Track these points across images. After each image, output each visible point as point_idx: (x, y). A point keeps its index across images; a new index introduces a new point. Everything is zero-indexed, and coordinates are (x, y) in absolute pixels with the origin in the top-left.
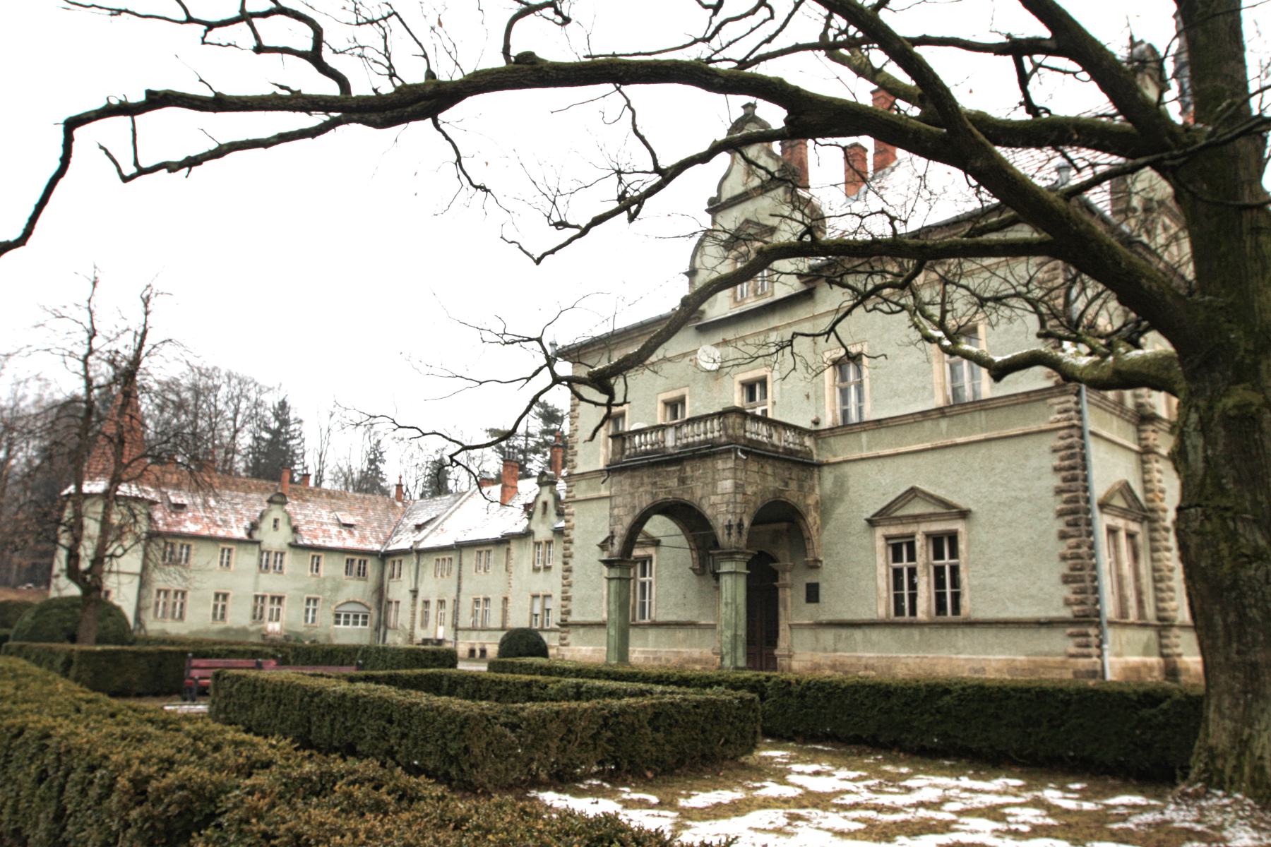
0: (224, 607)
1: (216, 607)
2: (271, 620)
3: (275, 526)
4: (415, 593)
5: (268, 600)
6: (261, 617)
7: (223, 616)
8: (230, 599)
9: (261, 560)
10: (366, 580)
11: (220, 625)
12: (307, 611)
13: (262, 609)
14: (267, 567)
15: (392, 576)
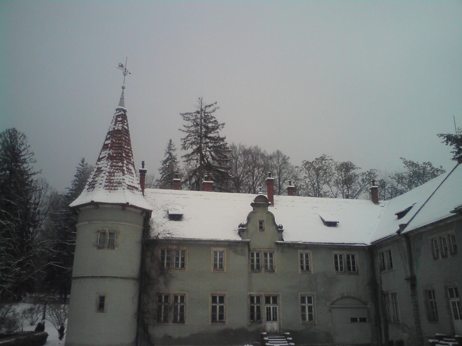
0: (221, 308)
1: (214, 308)
2: (268, 319)
3: (261, 228)
4: (412, 281)
5: (263, 300)
6: (259, 317)
7: (221, 317)
8: (226, 300)
9: (253, 261)
10: (357, 274)
11: (219, 327)
12: (303, 308)
13: (258, 308)
14: (258, 267)
15: (383, 268)
